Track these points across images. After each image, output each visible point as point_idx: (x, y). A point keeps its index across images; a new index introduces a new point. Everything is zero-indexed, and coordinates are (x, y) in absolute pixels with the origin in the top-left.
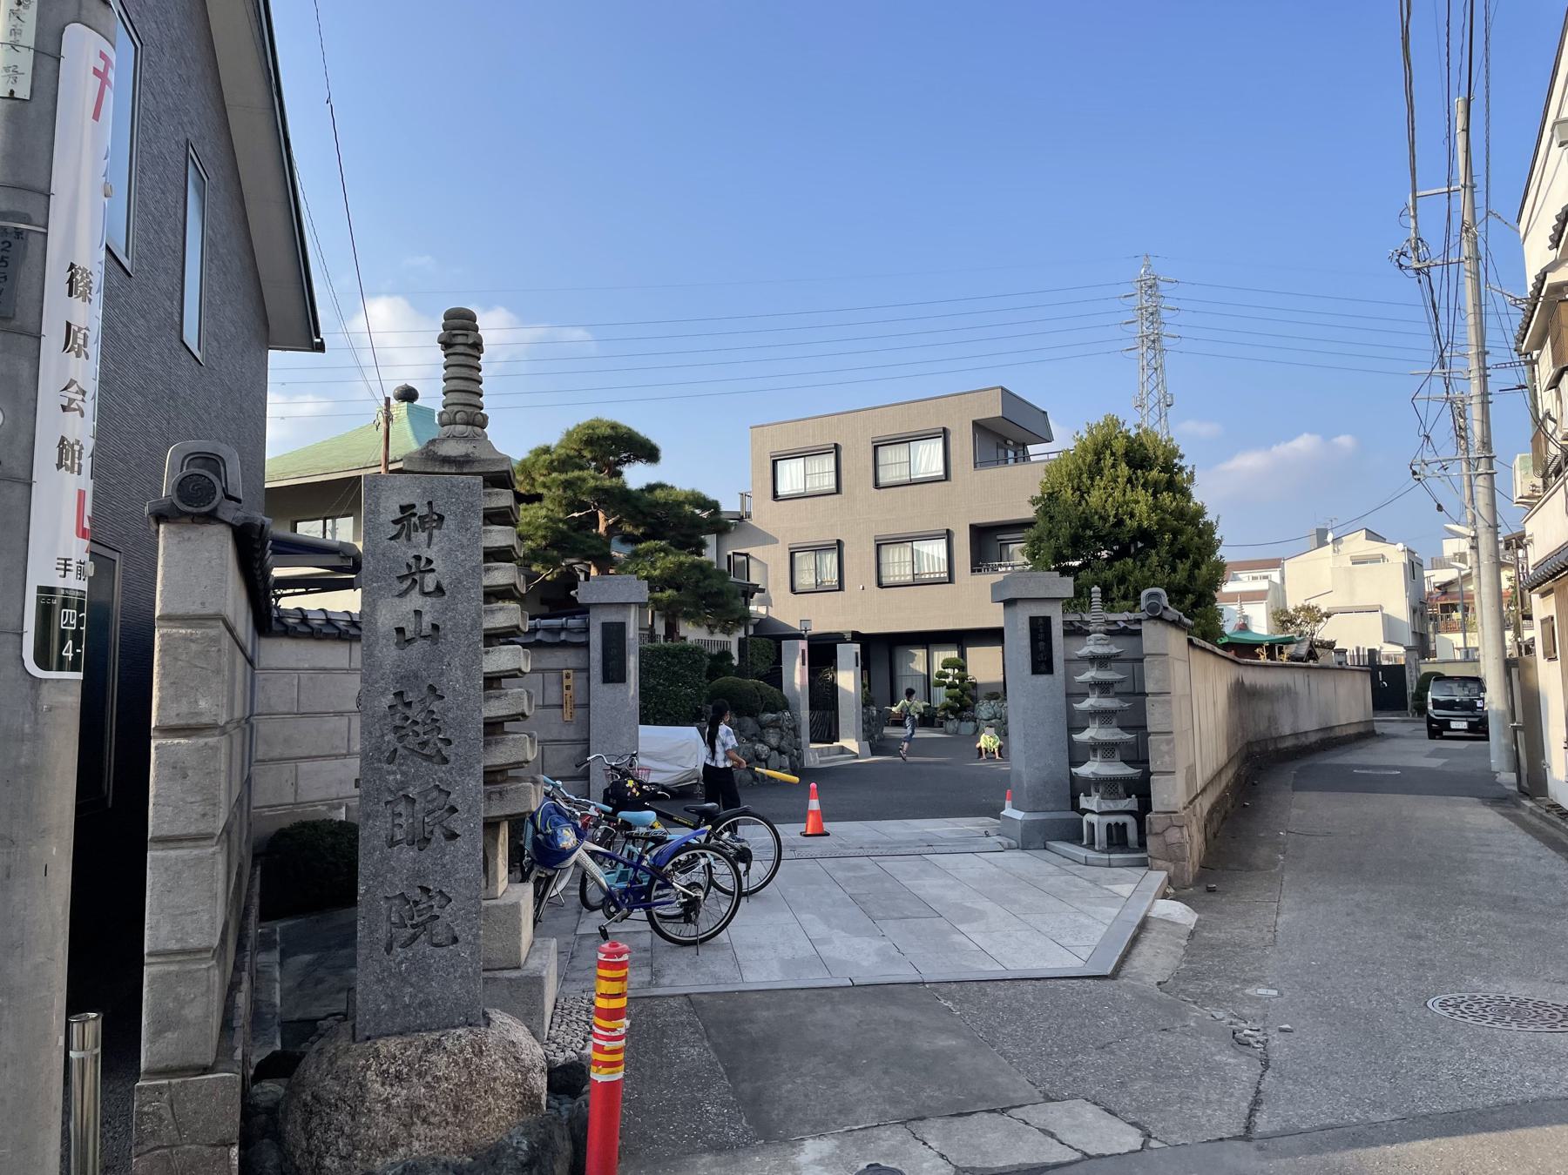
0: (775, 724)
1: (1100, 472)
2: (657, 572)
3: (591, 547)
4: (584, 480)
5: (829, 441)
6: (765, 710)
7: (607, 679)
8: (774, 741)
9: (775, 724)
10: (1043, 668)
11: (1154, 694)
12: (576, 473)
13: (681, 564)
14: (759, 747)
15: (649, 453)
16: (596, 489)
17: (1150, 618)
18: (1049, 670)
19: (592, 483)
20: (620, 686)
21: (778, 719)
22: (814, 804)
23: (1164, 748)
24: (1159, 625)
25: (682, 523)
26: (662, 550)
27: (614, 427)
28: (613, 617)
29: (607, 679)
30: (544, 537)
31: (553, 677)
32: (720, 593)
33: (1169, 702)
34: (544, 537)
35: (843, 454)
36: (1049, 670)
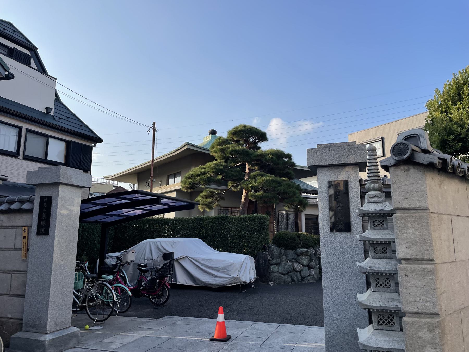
0: (305, 254)
1: (461, 100)
2: (256, 184)
3: (233, 175)
4: (228, 148)
5: (379, 137)
6: (302, 247)
7: (39, 233)
8: (305, 262)
9: (305, 254)
10: (342, 227)
11: (408, 260)
12: (226, 146)
13: (267, 181)
14: (296, 265)
15: (263, 137)
16: (232, 151)
17: (398, 164)
18: (347, 228)
19: (231, 149)
20: (45, 237)
21: (307, 252)
22: (221, 318)
23: (426, 335)
24: (413, 172)
25: (279, 164)
26: (259, 175)
27: (245, 126)
28: (46, 193)
29: (39, 233)
30: (213, 172)
31: (19, 230)
32: (285, 193)
33: (433, 272)
34: (213, 172)
35: (385, 141)
36: (347, 228)
